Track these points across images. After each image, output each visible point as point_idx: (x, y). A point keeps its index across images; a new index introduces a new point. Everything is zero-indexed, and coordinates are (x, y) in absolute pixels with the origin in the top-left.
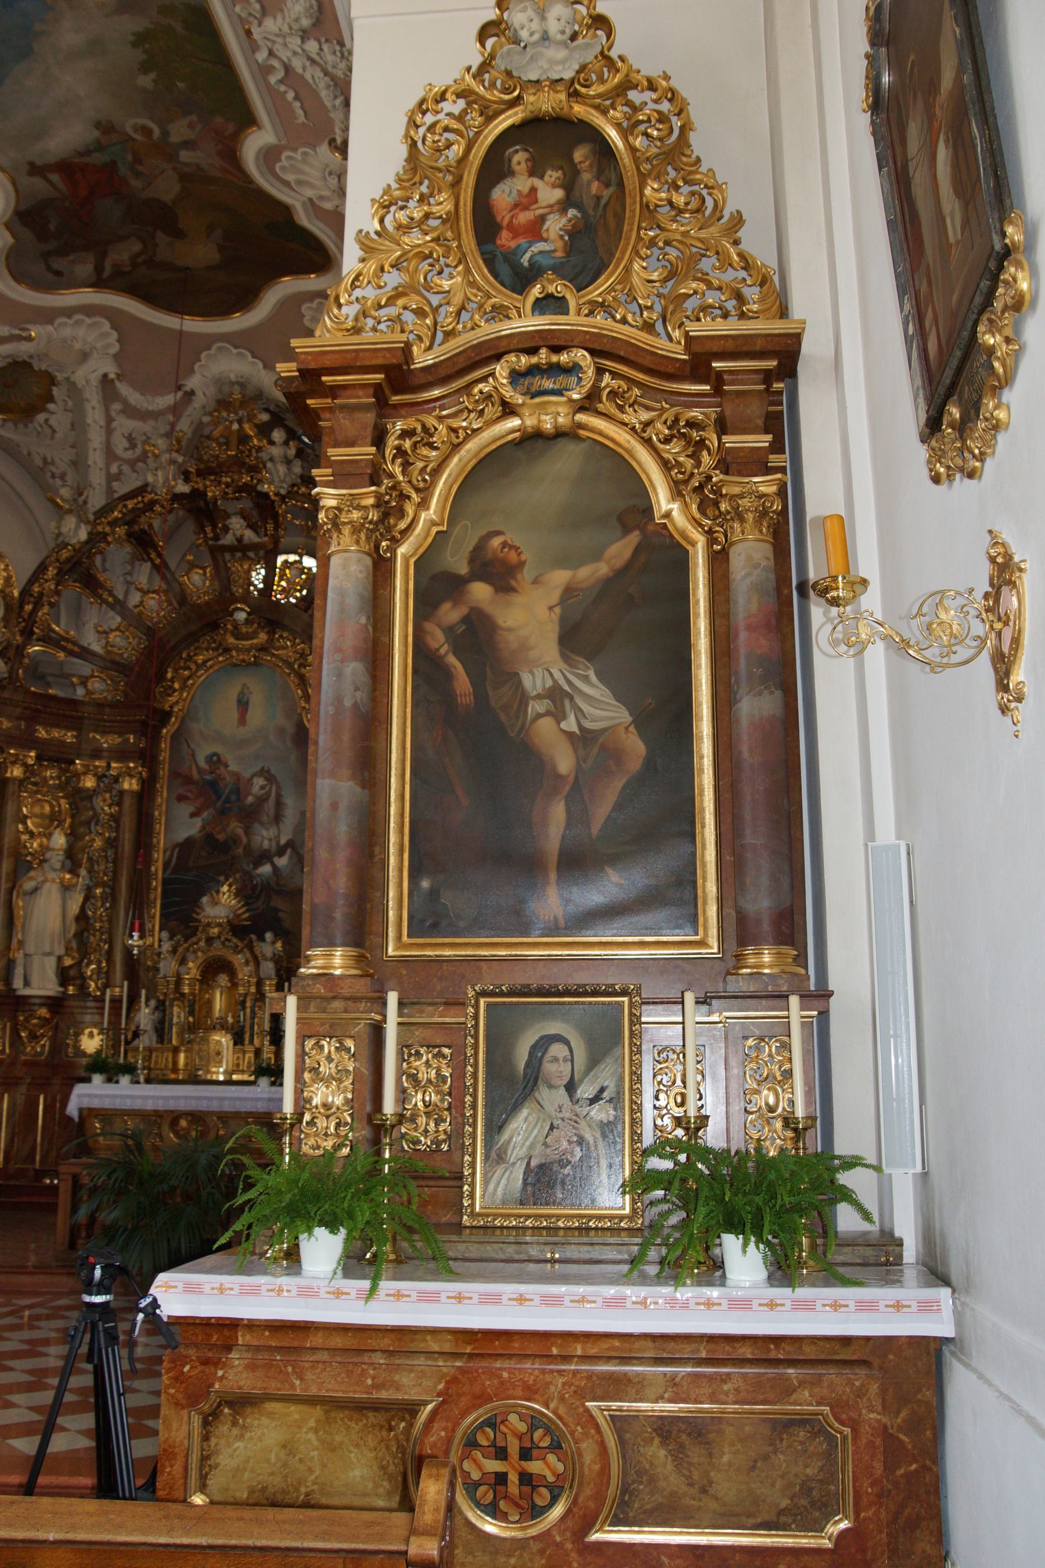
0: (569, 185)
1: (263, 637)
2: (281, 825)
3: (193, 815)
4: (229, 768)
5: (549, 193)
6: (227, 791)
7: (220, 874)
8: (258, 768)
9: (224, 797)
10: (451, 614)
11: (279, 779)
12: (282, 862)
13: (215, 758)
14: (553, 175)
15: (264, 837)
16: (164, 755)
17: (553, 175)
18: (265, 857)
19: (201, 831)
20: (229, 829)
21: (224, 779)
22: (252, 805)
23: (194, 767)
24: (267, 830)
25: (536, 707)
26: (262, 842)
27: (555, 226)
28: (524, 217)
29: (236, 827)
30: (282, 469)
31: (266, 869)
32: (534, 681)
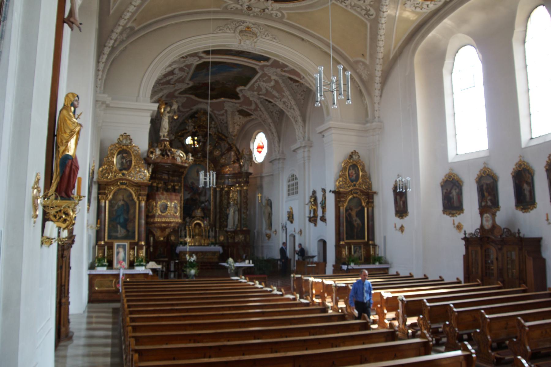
0: (355, 171)
1: (202, 159)
3: (189, 194)
5: (354, 172)
10: (348, 213)
12: (206, 204)
14: (354, 170)
15: (203, 199)
16: (183, 182)
17: (354, 170)
18: (203, 202)
25: (354, 221)
27: (354, 176)
28: (352, 174)
29: (197, 197)
30: (214, 130)
31: (203, 205)
32: (354, 219)
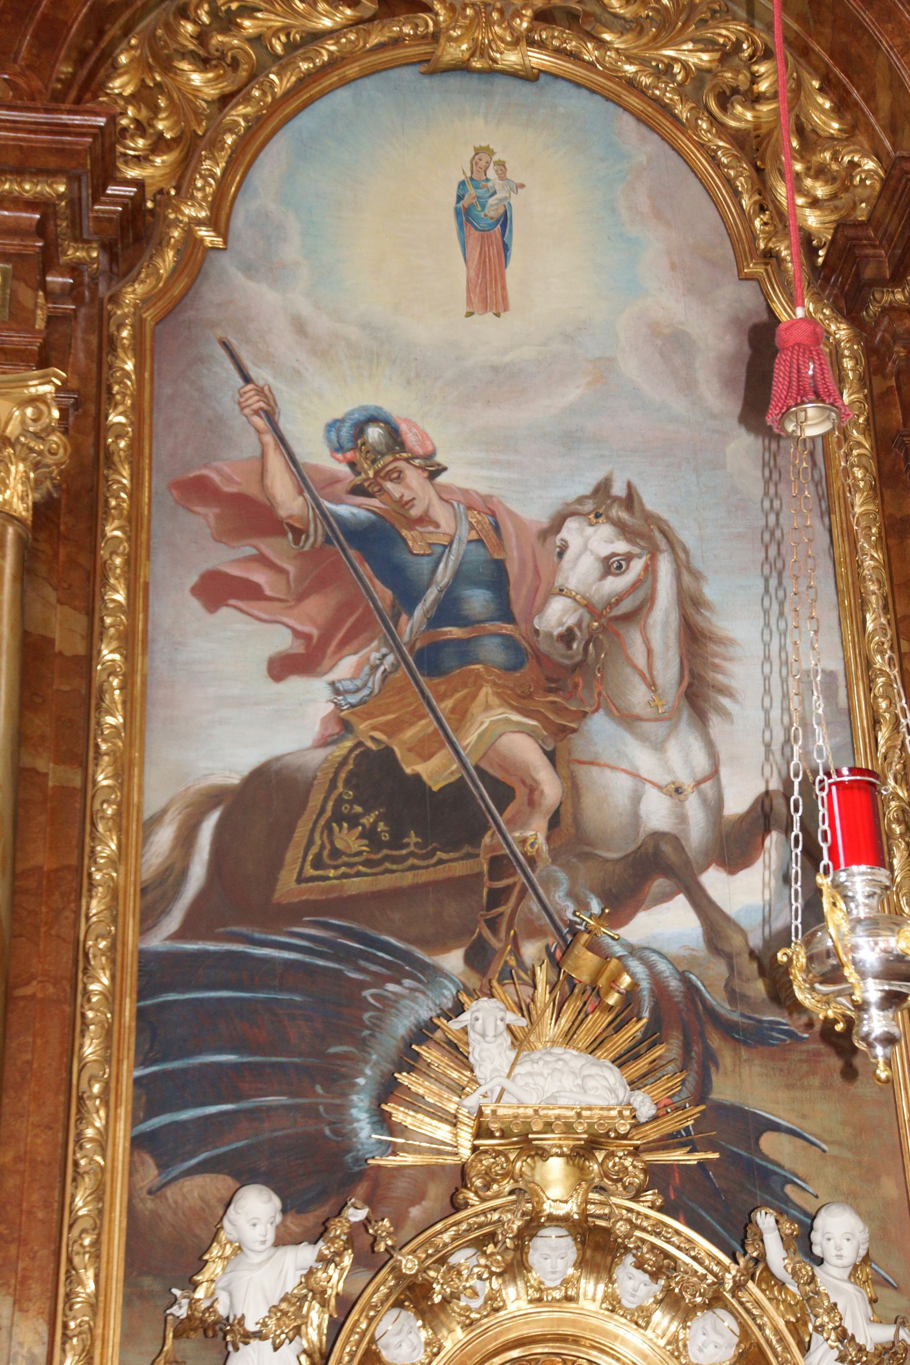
2: (716, 725)
4: (442, 479)
6: (444, 575)
7: (442, 944)
8: (584, 485)
9: (432, 595)
11: (686, 535)
13: (374, 433)
19: (324, 742)
20: (469, 739)
21: (425, 519)
22: (568, 637)
23: (276, 463)
24: (659, 747)
26: (636, 799)
